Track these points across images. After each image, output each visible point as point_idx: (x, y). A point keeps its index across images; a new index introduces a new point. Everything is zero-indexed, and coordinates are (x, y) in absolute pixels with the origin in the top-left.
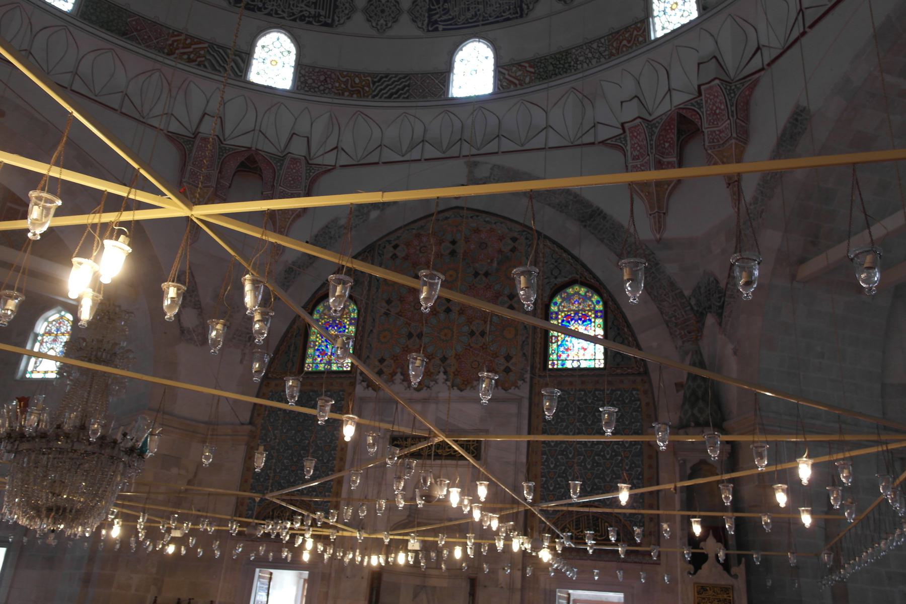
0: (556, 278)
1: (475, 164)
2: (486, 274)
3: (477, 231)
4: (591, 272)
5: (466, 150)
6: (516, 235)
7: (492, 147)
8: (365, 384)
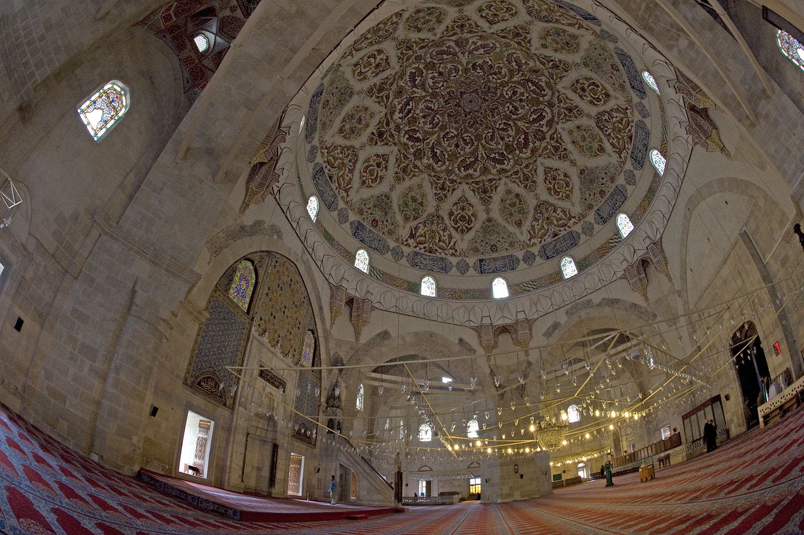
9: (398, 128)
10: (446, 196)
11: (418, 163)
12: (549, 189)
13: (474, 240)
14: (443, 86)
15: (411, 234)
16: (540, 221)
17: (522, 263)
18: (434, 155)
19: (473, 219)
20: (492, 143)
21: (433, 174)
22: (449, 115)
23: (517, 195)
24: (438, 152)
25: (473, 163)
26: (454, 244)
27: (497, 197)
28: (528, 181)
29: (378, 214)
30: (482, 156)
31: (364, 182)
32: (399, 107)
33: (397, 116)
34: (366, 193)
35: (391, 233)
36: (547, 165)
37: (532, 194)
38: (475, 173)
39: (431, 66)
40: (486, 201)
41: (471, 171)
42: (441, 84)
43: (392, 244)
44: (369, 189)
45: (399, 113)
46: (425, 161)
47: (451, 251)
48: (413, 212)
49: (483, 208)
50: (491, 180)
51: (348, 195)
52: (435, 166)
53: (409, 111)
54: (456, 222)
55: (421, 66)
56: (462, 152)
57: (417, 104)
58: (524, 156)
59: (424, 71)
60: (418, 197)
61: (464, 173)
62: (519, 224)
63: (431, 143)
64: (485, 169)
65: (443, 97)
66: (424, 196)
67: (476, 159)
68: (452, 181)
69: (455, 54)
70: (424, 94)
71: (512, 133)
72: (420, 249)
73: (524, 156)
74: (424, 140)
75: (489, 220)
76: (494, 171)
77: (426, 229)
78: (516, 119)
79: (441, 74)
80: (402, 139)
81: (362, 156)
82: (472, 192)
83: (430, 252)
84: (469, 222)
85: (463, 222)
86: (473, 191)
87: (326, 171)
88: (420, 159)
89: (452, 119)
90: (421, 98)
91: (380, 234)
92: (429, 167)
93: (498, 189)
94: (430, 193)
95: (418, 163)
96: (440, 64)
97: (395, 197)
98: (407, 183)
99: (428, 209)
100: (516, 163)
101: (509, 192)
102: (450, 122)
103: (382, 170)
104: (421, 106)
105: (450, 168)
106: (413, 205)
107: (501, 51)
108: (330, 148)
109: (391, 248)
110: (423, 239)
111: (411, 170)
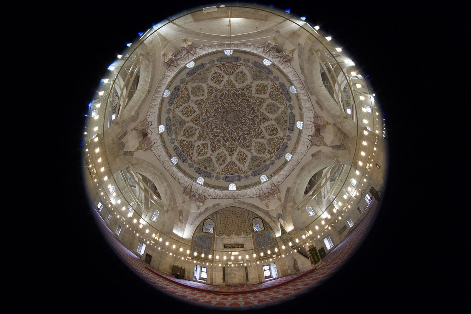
1: (235, 200)
2: (240, 217)
4: (259, 216)
5: (234, 198)
7: (238, 197)
9: (232, 145)
10: (263, 134)
11: (248, 141)
12: (264, 93)
13: (281, 129)
14: (221, 127)
15: (269, 153)
16: (277, 99)
17: (292, 111)
18: (247, 134)
19: (274, 126)
20: (247, 112)
21: (253, 136)
22: (234, 126)
23: (267, 106)
24: (246, 132)
25: (253, 120)
26: (280, 137)
27: (268, 114)
28: (262, 101)
29: (256, 163)
30: (251, 117)
31: (243, 163)
32: (224, 142)
33: (227, 144)
34: (247, 164)
35: (265, 161)
36: (255, 93)
37: (267, 100)
38: (257, 121)
39: (212, 130)
40: (268, 119)
41: (256, 122)
42: (220, 127)
43: (268, 163)
44: (247, 162)
45: (227, 143)
46: (248, 138)
47: (282, 140)
48: (264, 149)
49: (271, 121)
50: (261, 115)
51: (243, 171)
52: (251, 135)
53: (228, 139)
54: (273, 134)
55: (211, 133)
56: (249, 124)
57: (226, 136)
58: (252, 101)
59: (213, 132)
60: (259, 145)
61: (256, 125)
62: (278, 108)
63: (242, 134)
64: (256, 117)
65: (226, 127)
66: (260, 143)
67: (252, 119)
68: (258, 130)
69: (209, 122)
70: (222, 133)
71: (243, 105)
72: (276, 152)
73: (252, 101)
74: (240, 136)
75: (275, 120)
76: (258, 113)
77: (271, 147)
78: (237, 103)
79: (216, 127)
80: (236, 144)
81: (234, 160)
82: (264, 124)
83: (279, 149)
84: (274, 128)
85: (273, 131)
86: (264, 123)
87: (229, 175)
88: (246, 139)
89: (235, 125)
90: (224, 134)
91: (262, 166)
92: (251, 137)
93: (264, 113)
94: (260, 140)
95: (248, 141)
96: (212, 127)
97: (255, 154)
98: (253, 147)
99: (265, 143)
100: (255, 104)
101: (266, 109)
102: (236, 126)
103: (244, 155)
104: (227, 135)
105: (253, 129)
106: (261, 149)
107: (208, 107)
108: (223, 170)
109: (269, 164)
110: (273, 149)
111: (249, 144)
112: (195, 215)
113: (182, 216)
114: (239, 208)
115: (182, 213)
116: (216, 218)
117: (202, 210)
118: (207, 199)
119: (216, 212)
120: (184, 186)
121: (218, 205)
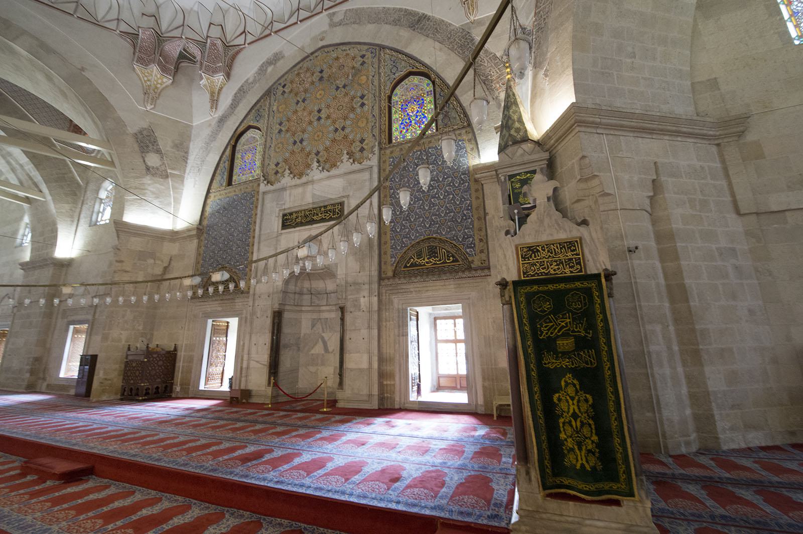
0: (394, 74)
3: (337, 59)
6: (364, 53)
8: (265, 182)
112: (207, 132)
113: (158, 151)
114: (347, 47)
115: (155, 142)
116: (269, 115)
117: (225, 101)
118: (239, 50)
119: (268, 93)
120: (123, 27)
121: (276, 58)
